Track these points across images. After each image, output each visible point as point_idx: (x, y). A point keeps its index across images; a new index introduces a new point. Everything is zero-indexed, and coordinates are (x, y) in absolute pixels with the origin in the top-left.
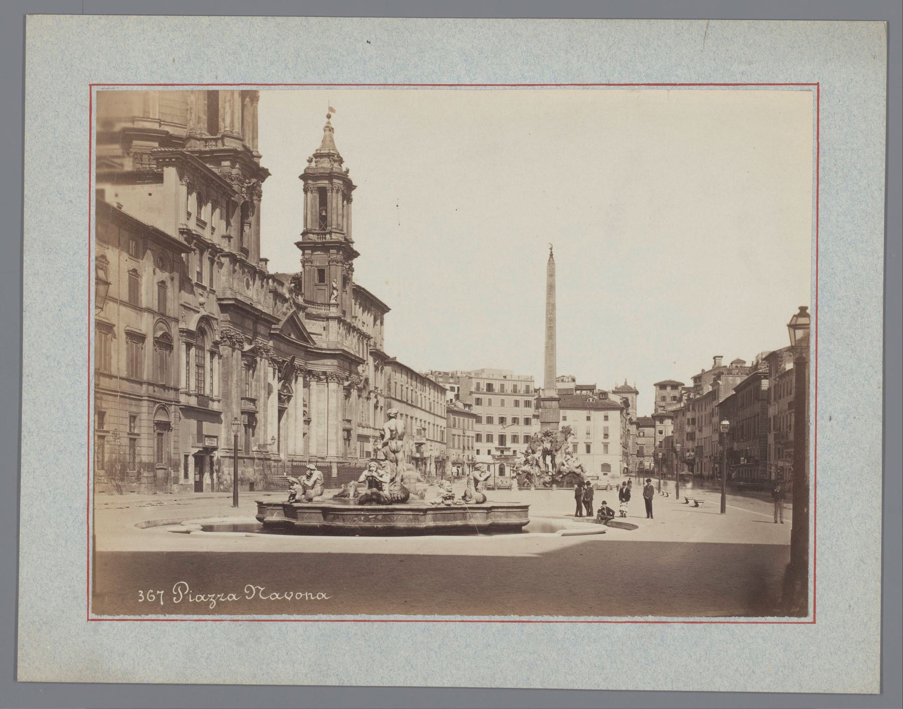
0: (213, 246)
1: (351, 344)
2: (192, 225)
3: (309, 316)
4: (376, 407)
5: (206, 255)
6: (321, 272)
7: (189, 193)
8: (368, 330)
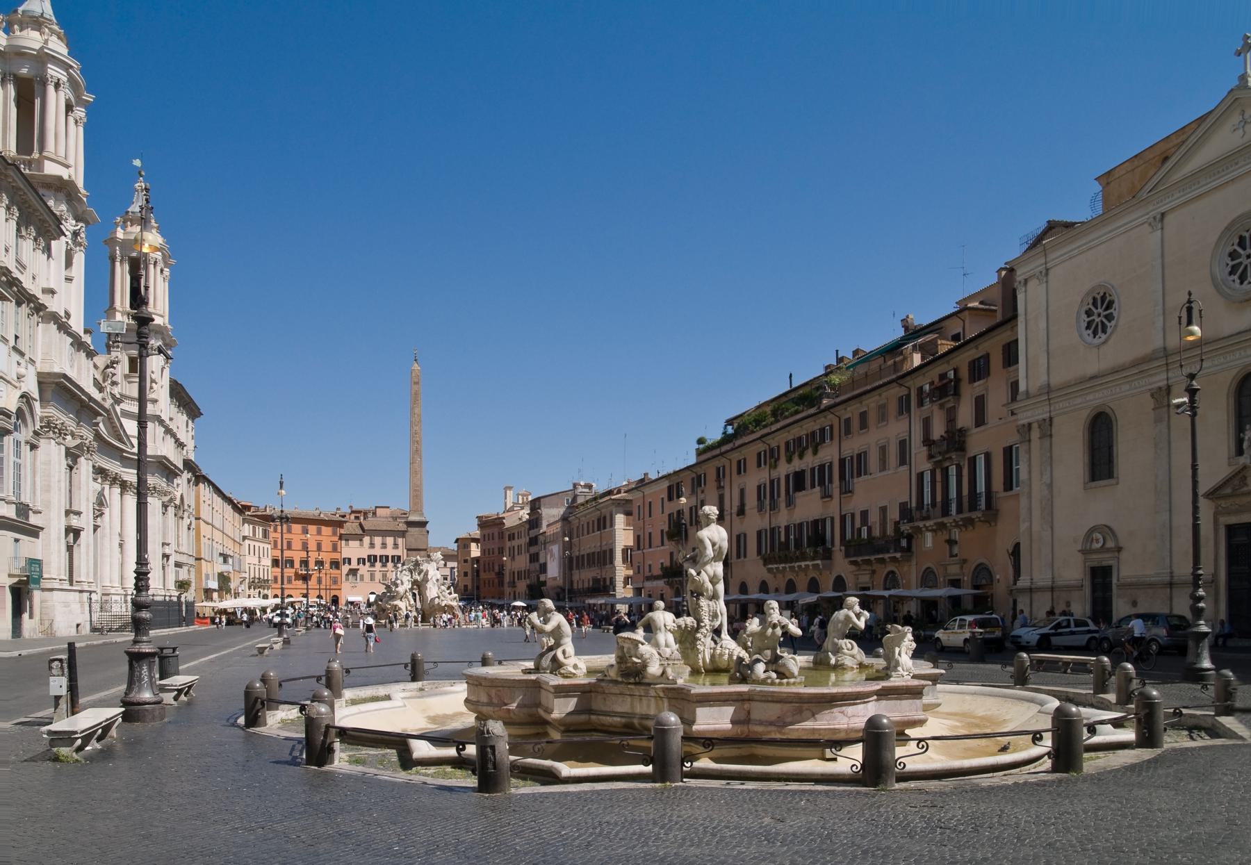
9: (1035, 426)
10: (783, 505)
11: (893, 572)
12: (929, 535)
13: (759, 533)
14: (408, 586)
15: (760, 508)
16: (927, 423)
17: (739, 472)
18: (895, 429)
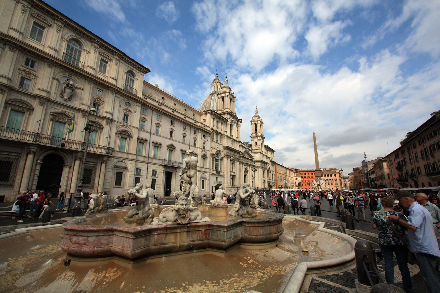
0: (221, 134)
1: (265, 159)
2: (215, 128)
3: (252, 152)
4: (273, 174)
5: (219, 135)
6: (256, 143)
7: (214, 120)
8: (269, 156)
10: (430, 156)
14: (316, 185)
15: (423, 158)
17: (414, 148)
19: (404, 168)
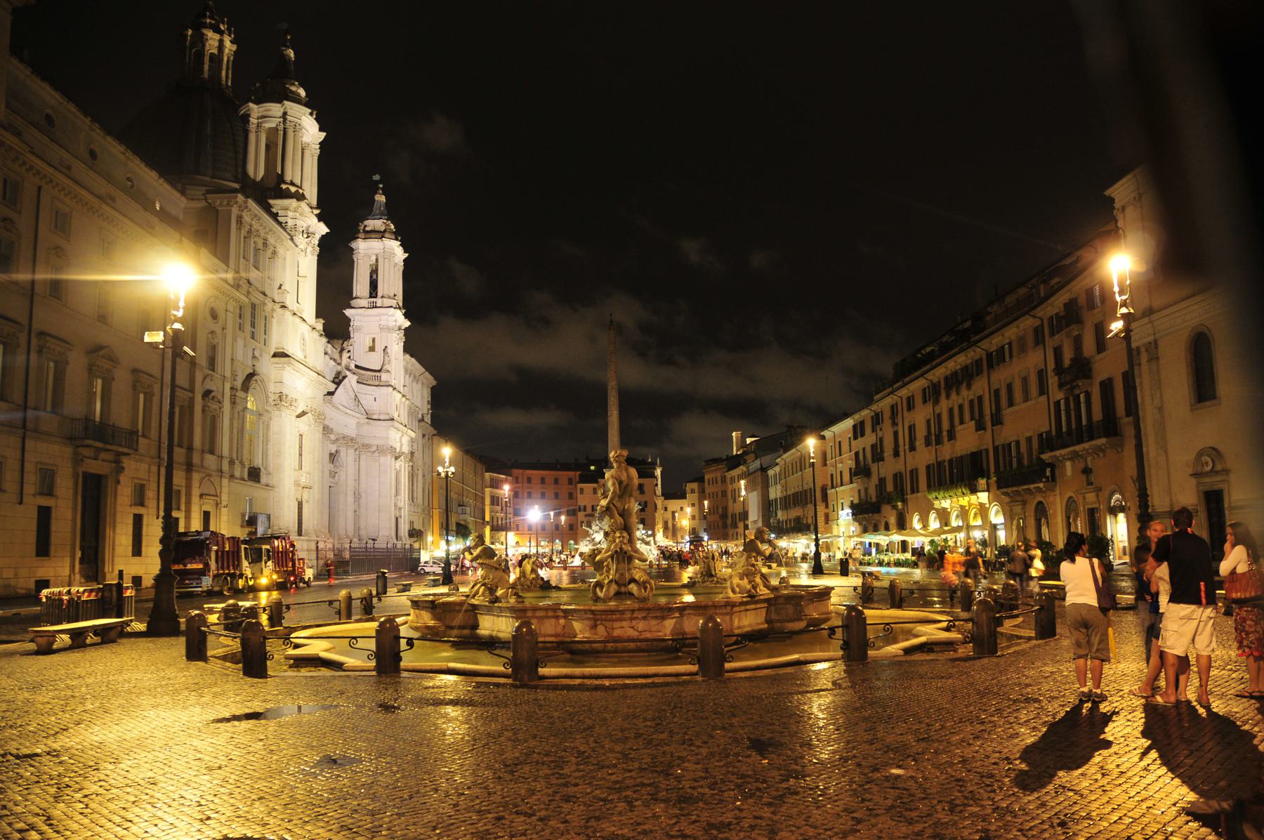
9: (1143, 349)
10: (946, 439)
11: (1040, 503)
12: (1068, 464)
13: (928, 467)
15: (928, 444)
16: (1058, 352)
17: (909, 409)
18: (1034, 360)
19: (874, 468)
